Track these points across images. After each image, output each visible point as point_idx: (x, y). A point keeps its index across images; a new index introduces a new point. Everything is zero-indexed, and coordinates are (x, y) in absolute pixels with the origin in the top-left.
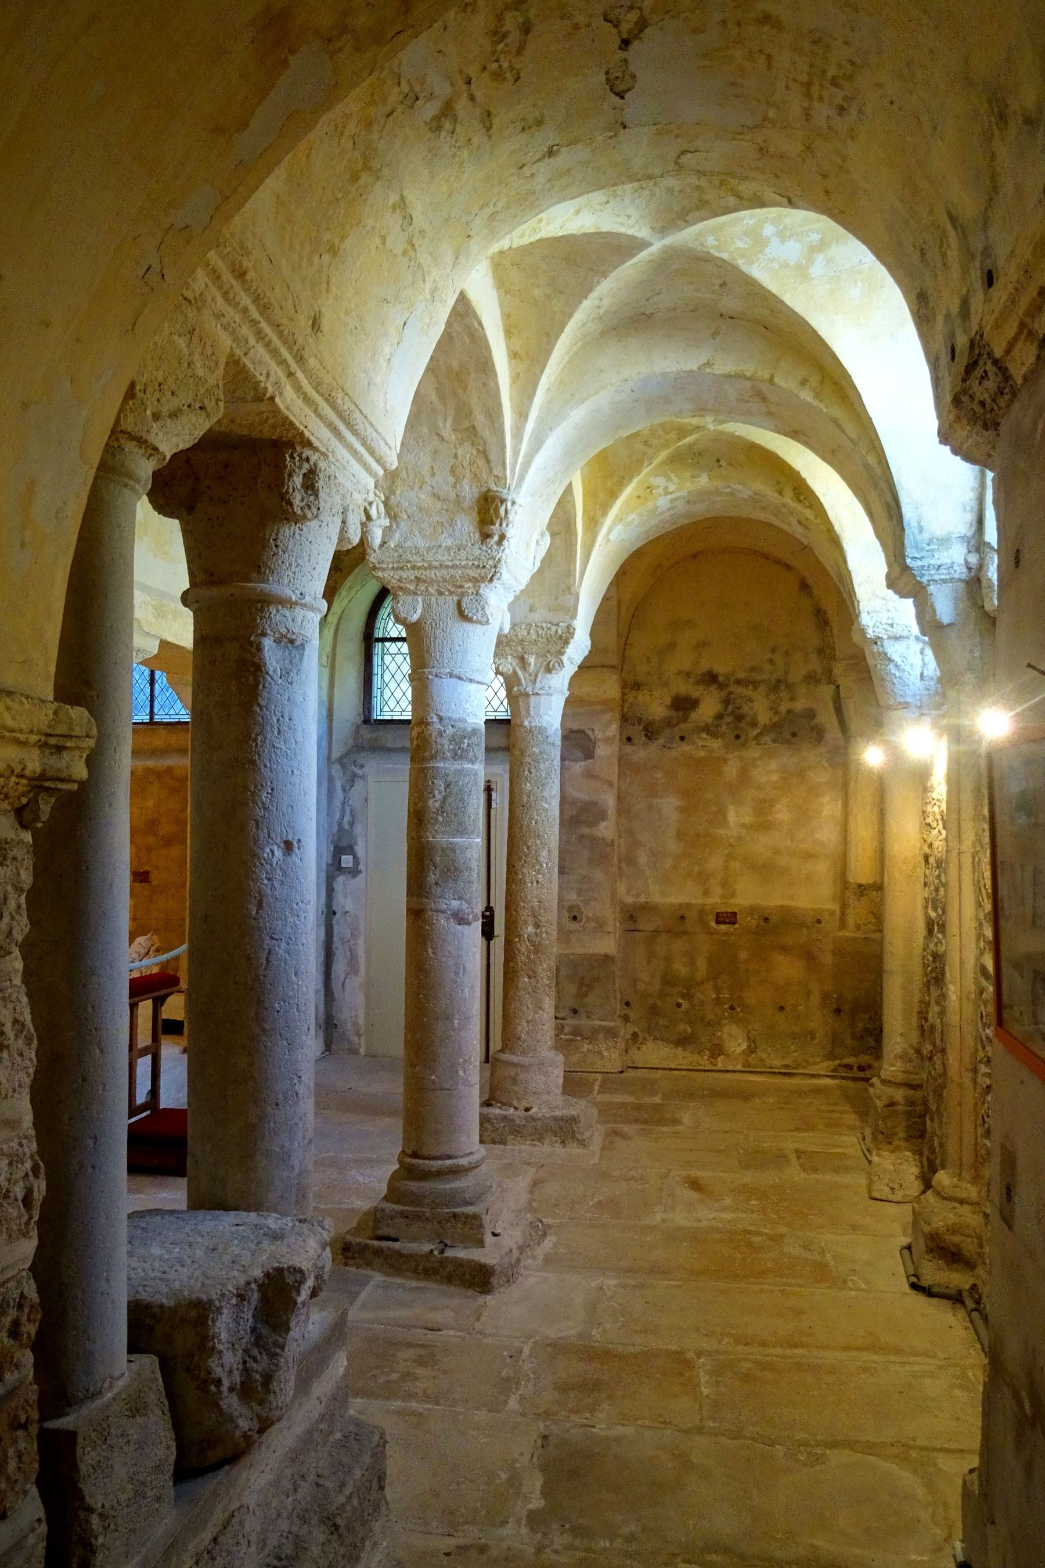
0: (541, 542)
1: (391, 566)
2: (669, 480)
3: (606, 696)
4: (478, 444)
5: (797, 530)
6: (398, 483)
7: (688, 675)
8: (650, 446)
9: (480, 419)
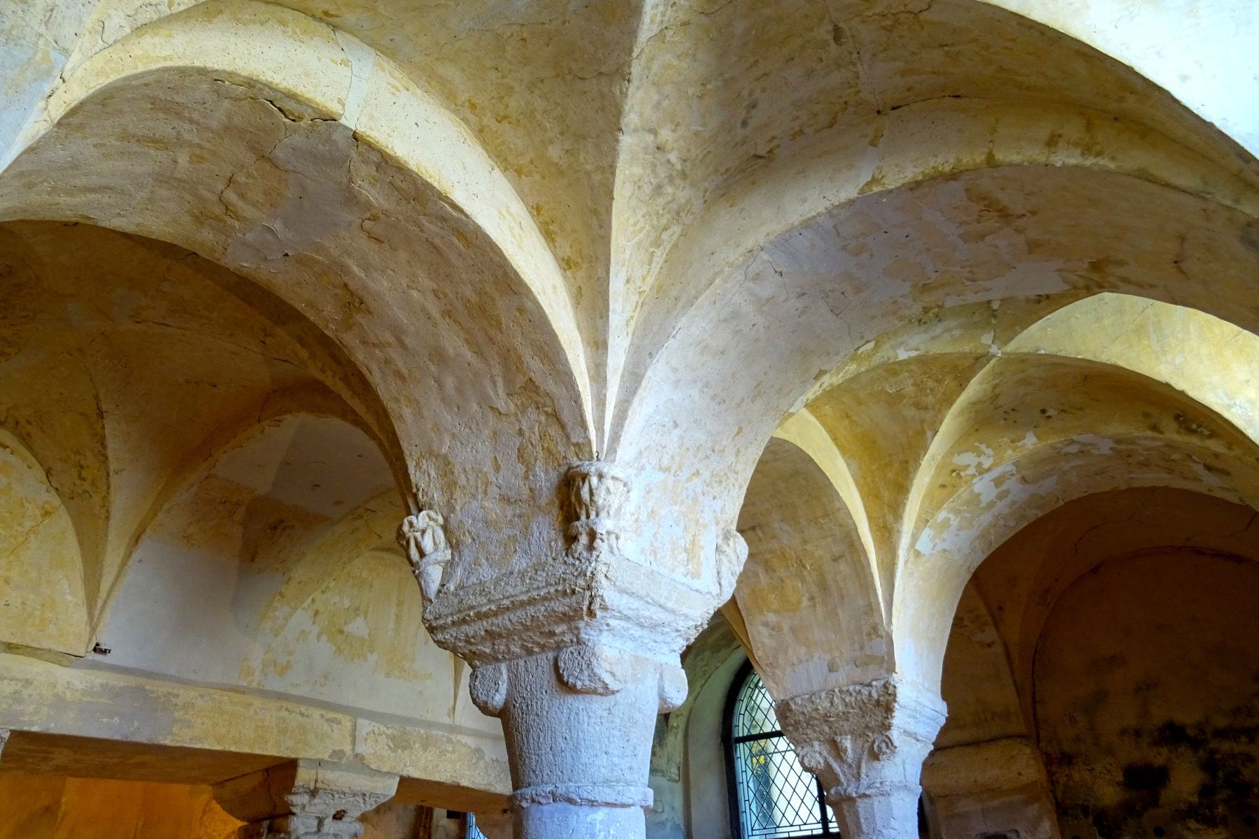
0: (725, 548)
1: (450, 619)
2: (980, 453)
3: (1023, 780)
4: (545, 405)
5: (1210, 483)
6: (458, 494)
7: (1138, 733)
8: (926, 408)
9: (535, 365)
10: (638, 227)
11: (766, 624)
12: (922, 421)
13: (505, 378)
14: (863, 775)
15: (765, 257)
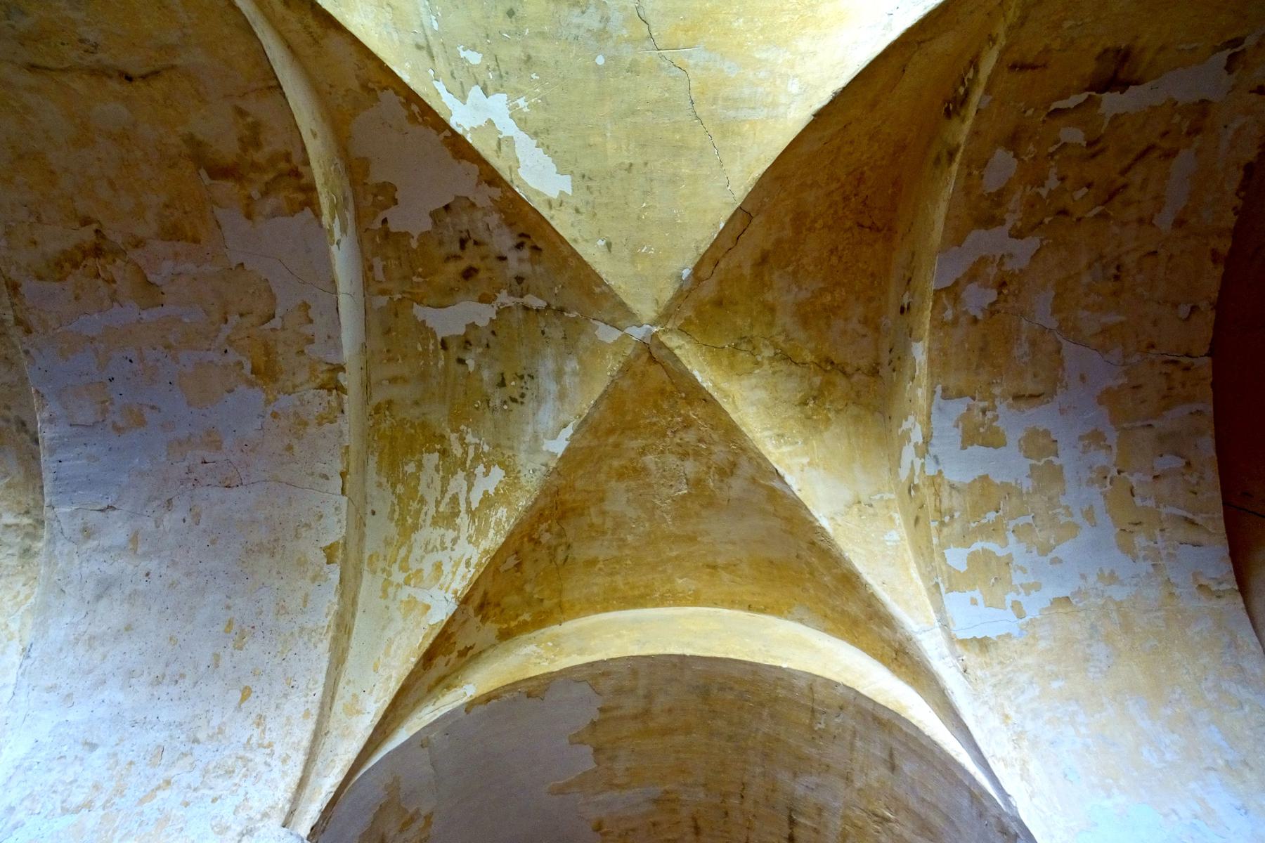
10: (21, 597)
12: (754, 480)
15: (67, 509)
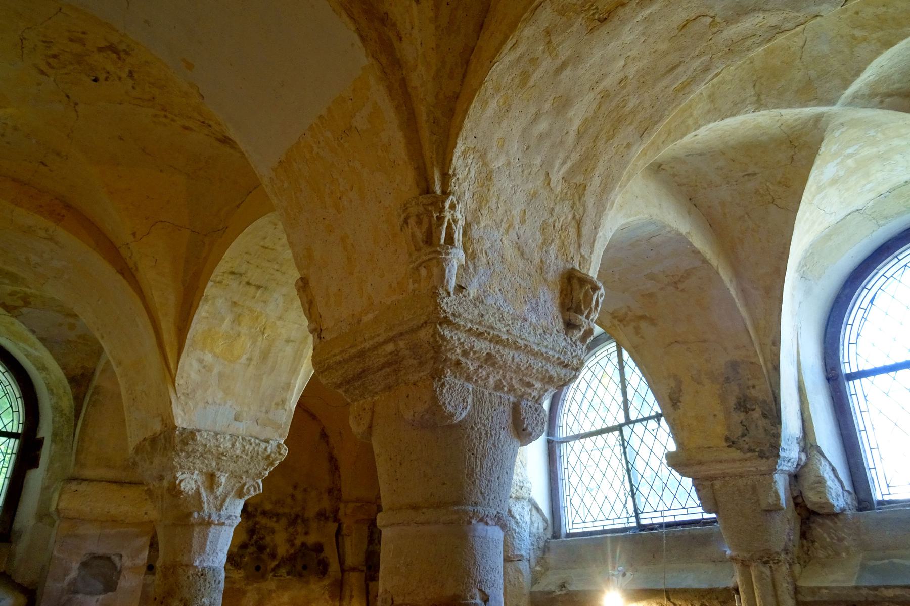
11: (201, 361)
13: (573, 166)
14: (224, 508)
